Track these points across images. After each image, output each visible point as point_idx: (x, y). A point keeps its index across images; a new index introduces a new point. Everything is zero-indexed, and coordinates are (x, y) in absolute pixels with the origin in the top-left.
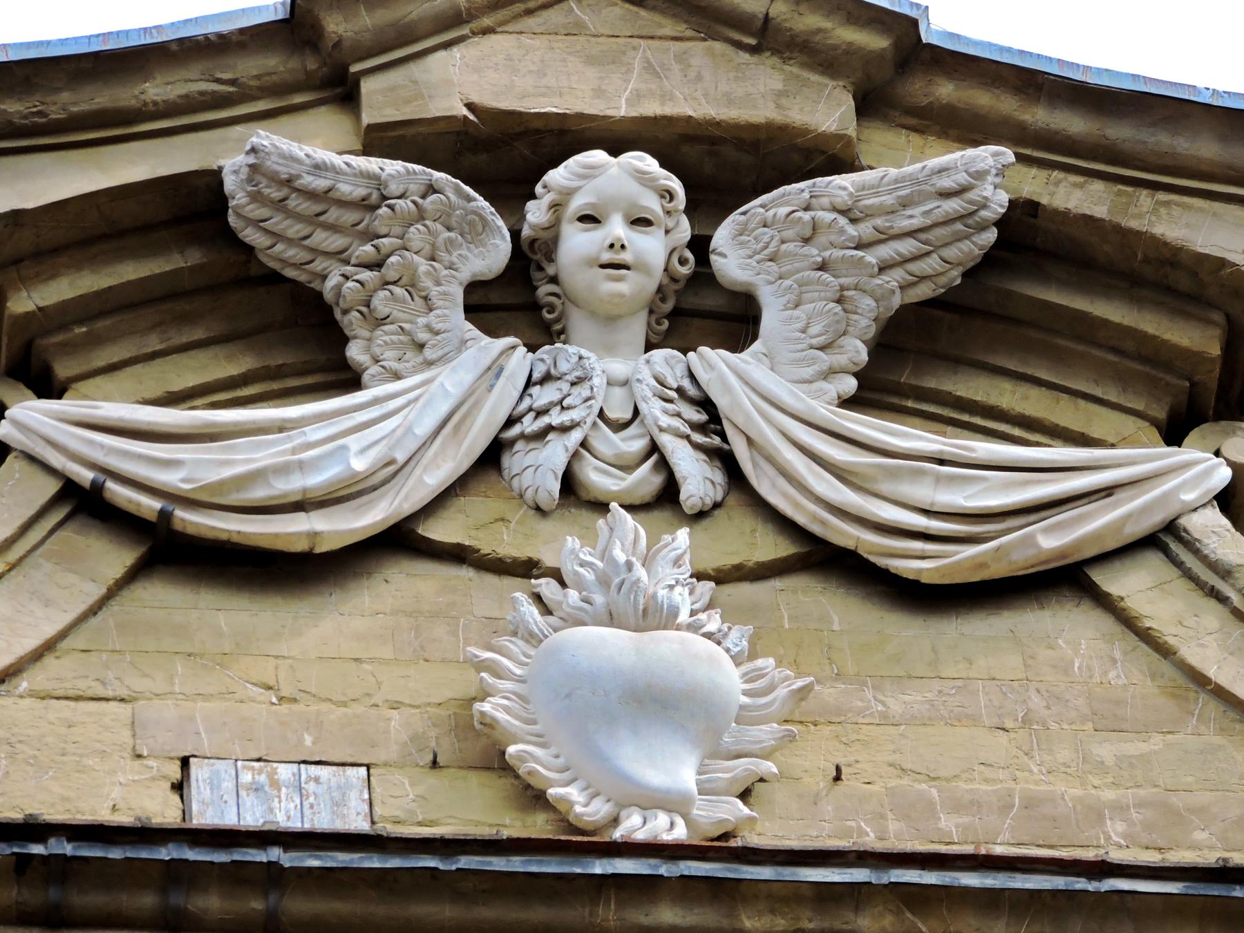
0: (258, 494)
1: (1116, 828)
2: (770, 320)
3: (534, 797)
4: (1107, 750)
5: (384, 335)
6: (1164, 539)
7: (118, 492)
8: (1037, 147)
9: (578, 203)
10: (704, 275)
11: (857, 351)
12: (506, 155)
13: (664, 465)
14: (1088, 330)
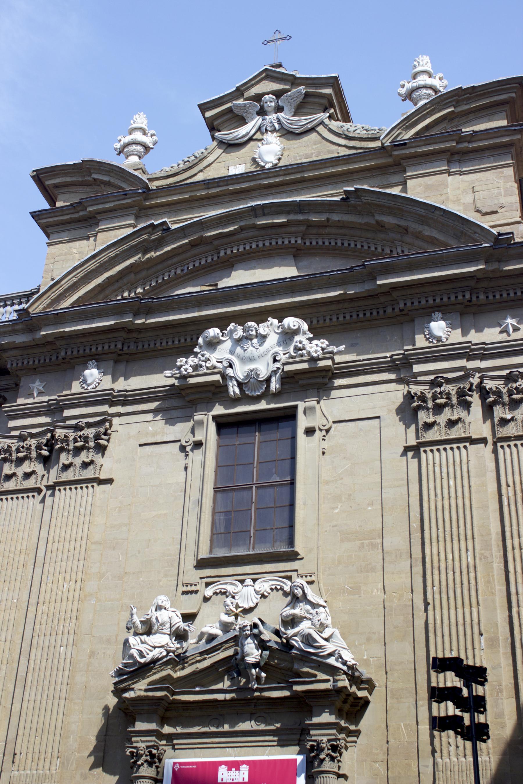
0: (235, 138)
1: (314, 155)
2: (285, 109)
3: (258, 164)
4: (314, 147)
5: (249, 118)
6: (322, 123)
7: (224, 141)
8: (308, 85)
9: (265, 101)
10: (279, 105)
11: (293, 110)
12: (258, 98)
13: (274, 126)
14: (315, 103)
